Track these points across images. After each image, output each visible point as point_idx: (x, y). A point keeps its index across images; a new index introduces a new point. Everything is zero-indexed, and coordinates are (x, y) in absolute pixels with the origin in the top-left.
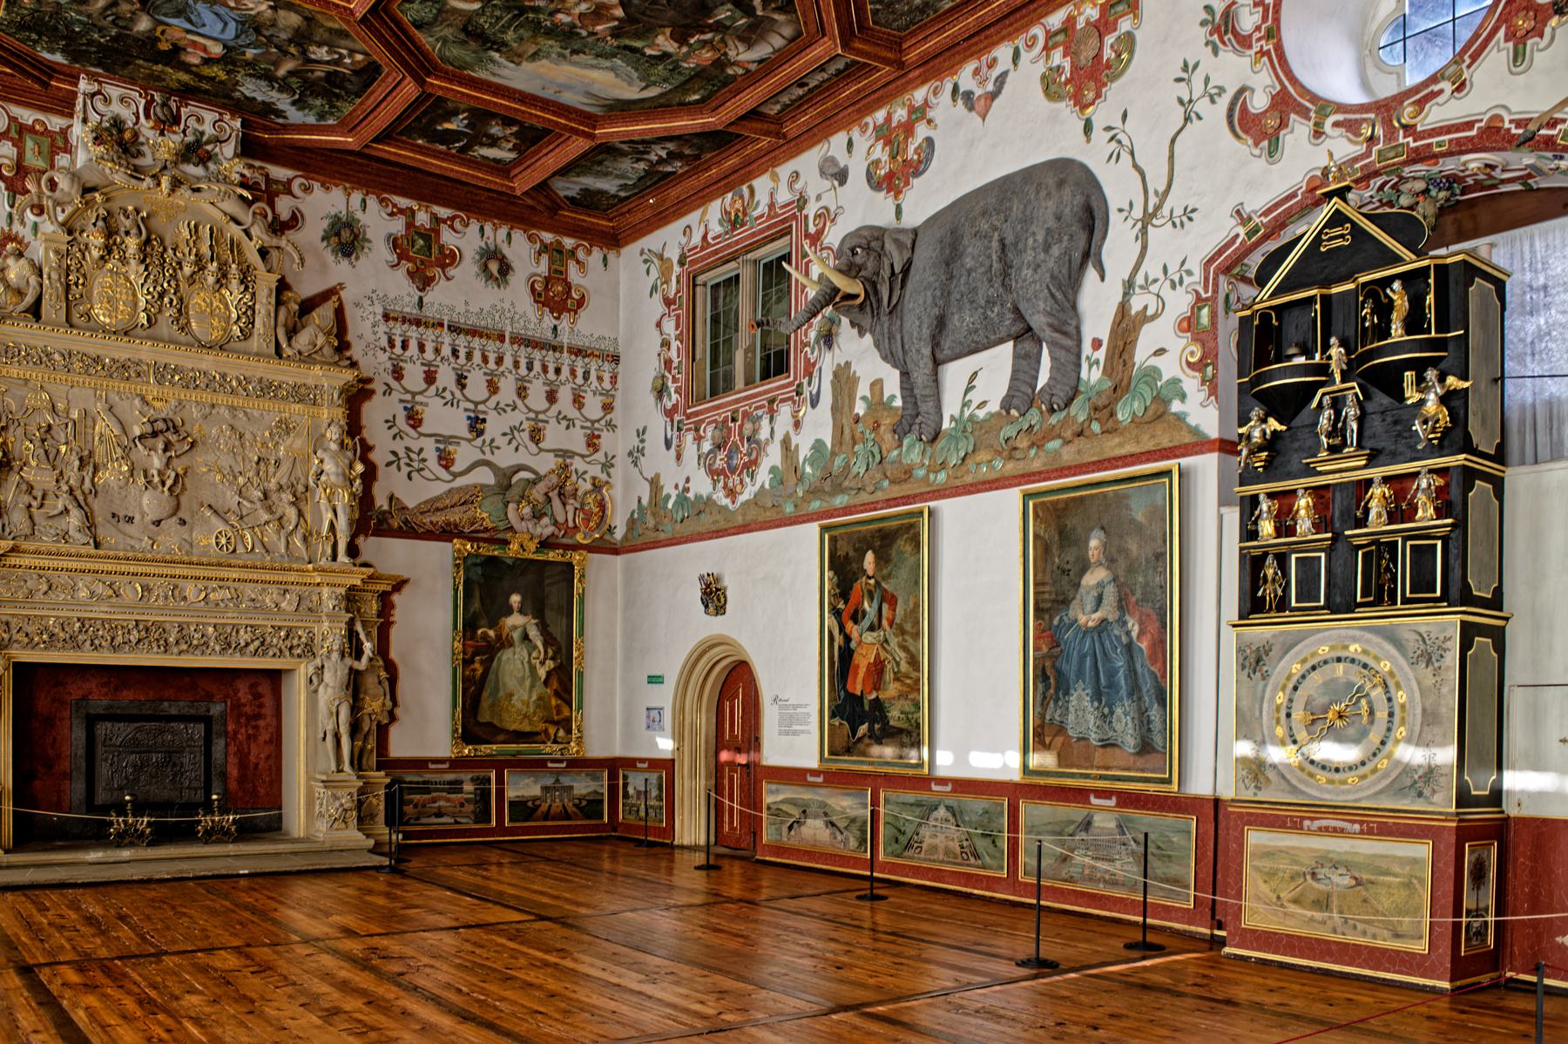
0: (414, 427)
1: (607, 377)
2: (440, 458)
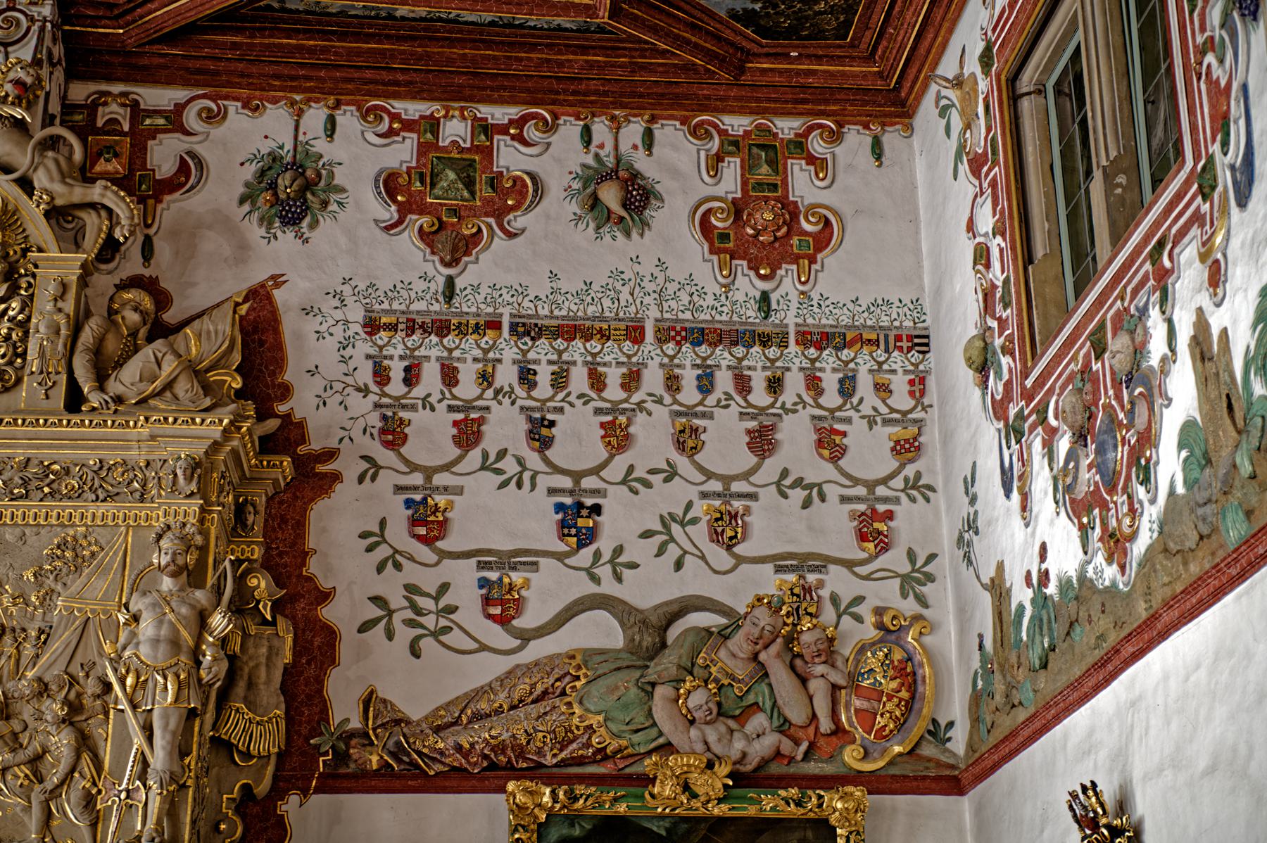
0: (426, 541)
1: (900, 383)
2: (487, 601)
